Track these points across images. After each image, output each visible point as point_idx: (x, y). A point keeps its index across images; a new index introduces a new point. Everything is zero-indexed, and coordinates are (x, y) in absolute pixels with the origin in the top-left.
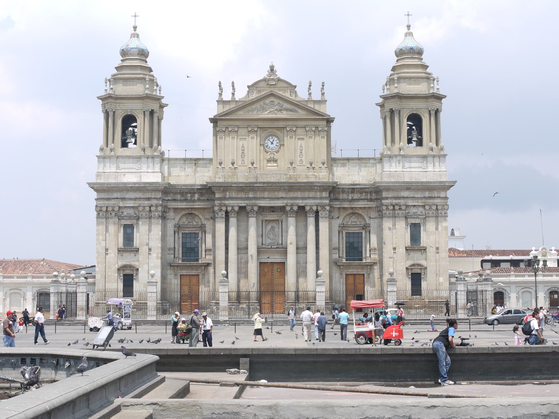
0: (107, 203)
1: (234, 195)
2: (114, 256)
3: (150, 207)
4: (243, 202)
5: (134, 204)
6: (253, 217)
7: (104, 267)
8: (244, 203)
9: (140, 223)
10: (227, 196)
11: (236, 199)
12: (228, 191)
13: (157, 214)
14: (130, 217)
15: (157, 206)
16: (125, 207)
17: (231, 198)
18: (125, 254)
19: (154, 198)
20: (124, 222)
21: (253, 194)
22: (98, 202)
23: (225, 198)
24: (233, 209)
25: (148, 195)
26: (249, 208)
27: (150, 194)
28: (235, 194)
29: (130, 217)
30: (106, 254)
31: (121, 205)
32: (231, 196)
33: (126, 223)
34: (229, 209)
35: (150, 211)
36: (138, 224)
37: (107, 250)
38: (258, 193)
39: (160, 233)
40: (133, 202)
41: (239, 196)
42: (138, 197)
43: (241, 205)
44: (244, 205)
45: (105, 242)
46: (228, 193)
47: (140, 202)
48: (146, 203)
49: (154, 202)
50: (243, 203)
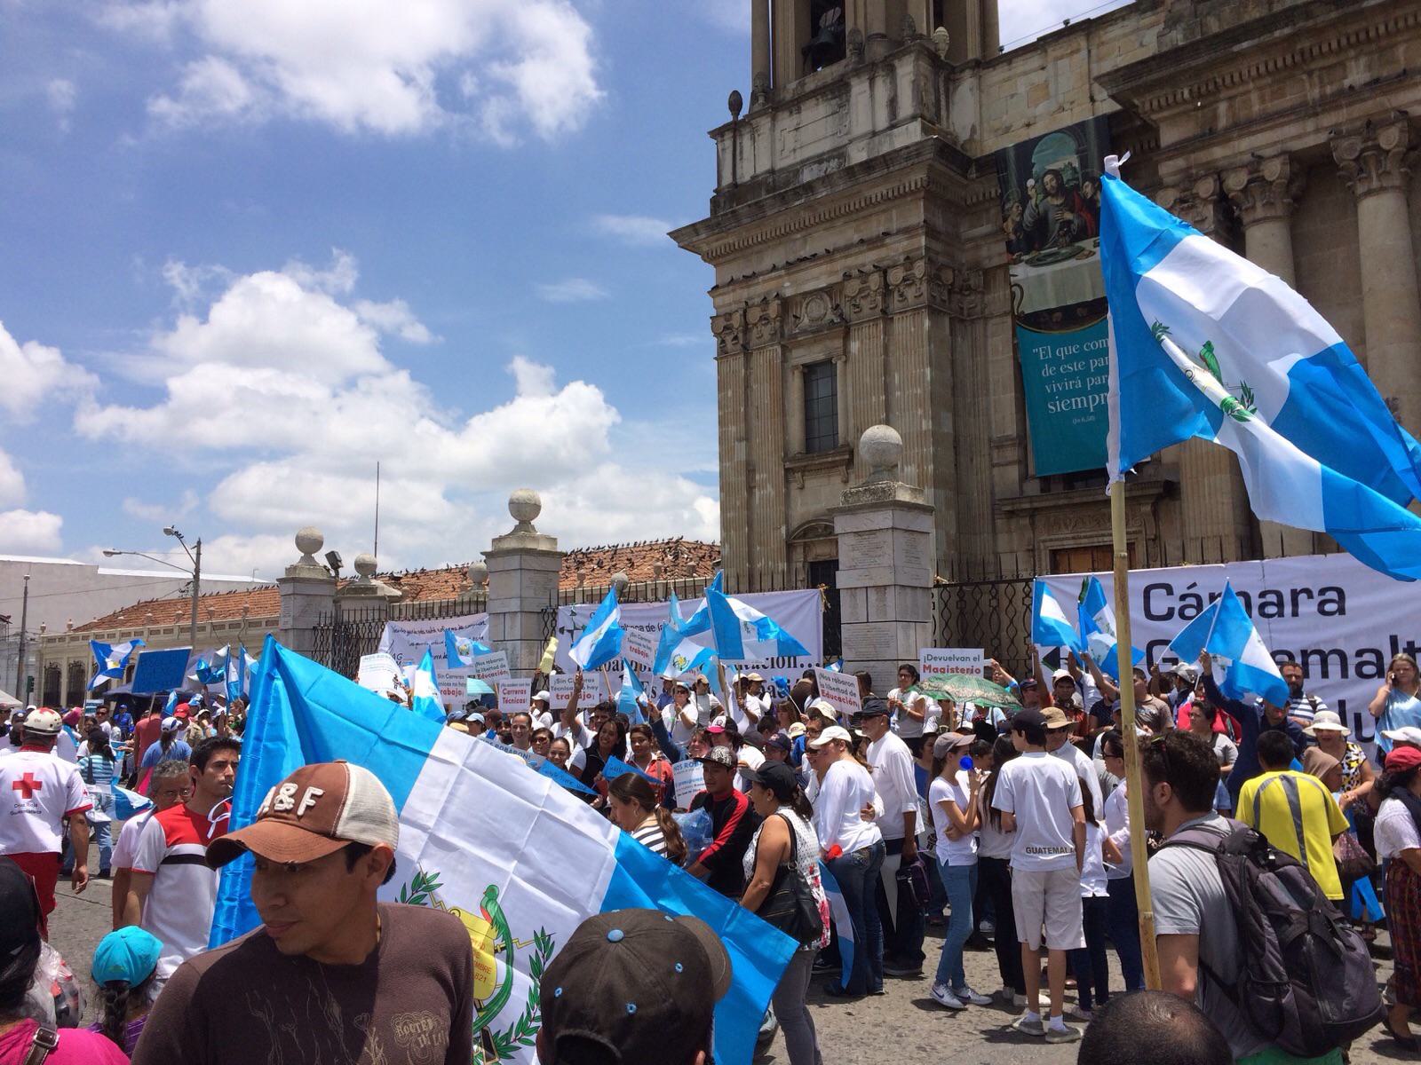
0: (743, 294)
1: (1256, 108)
2: (773, 493)
3: (885, 272)
4: (1310, 125)
5: (832, 273)
6: (1382, 189)
7: (745, 539)
8: (1317, 131)
9: (855, 346)
10: (1223, 122)
11: (1270, 119)
12: (1222, 96)
13: (910, 293)
14: (818, 332)
15: (909, 261)
16: (805, 294)
17: (1243, 127)
18: (812, 483)
19: (899, 232)
20: (803, 356)
21: (1369, 67)
22: (720, 300)
23: (1209, 136)
24: (1257, 180)
25: (875, 228)
26: (1346, 151)
27: (883, 217)
28: (1262, 100)
29: (818, 332)
30: (750, 489)
31: (788, 293)
32: (1243, 115)
33: (808, 360)
34: (1236, 182)
35: (887, 290)
36: (846, 352)
37: (750, 470)
38: (1401, 50)
39: (928, 371)
40: (824, 268)
41: (1290, 99)
42: (841, 242)
43: (1297, 145)
44: (1322, 138)
45: (744, 444)
46: (1223, 107)
47: (851, 261)
48: (869, 258)
49: (897, 248)
50: (1305, 135)
